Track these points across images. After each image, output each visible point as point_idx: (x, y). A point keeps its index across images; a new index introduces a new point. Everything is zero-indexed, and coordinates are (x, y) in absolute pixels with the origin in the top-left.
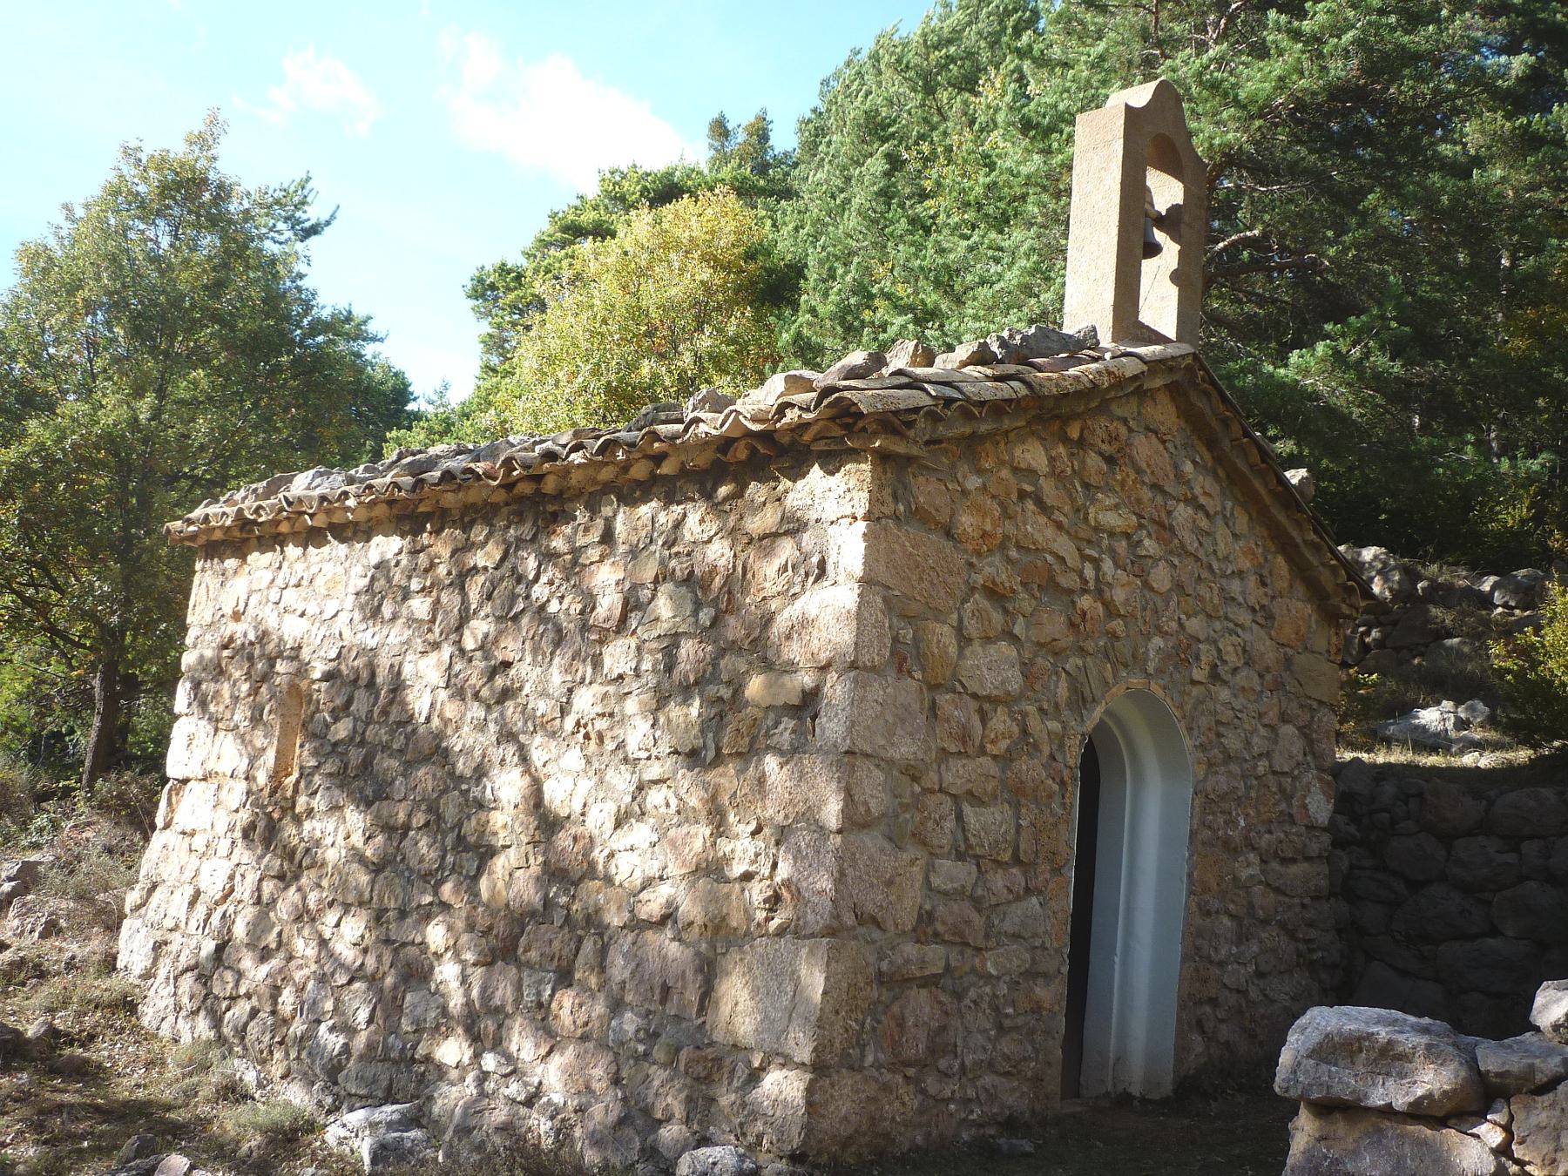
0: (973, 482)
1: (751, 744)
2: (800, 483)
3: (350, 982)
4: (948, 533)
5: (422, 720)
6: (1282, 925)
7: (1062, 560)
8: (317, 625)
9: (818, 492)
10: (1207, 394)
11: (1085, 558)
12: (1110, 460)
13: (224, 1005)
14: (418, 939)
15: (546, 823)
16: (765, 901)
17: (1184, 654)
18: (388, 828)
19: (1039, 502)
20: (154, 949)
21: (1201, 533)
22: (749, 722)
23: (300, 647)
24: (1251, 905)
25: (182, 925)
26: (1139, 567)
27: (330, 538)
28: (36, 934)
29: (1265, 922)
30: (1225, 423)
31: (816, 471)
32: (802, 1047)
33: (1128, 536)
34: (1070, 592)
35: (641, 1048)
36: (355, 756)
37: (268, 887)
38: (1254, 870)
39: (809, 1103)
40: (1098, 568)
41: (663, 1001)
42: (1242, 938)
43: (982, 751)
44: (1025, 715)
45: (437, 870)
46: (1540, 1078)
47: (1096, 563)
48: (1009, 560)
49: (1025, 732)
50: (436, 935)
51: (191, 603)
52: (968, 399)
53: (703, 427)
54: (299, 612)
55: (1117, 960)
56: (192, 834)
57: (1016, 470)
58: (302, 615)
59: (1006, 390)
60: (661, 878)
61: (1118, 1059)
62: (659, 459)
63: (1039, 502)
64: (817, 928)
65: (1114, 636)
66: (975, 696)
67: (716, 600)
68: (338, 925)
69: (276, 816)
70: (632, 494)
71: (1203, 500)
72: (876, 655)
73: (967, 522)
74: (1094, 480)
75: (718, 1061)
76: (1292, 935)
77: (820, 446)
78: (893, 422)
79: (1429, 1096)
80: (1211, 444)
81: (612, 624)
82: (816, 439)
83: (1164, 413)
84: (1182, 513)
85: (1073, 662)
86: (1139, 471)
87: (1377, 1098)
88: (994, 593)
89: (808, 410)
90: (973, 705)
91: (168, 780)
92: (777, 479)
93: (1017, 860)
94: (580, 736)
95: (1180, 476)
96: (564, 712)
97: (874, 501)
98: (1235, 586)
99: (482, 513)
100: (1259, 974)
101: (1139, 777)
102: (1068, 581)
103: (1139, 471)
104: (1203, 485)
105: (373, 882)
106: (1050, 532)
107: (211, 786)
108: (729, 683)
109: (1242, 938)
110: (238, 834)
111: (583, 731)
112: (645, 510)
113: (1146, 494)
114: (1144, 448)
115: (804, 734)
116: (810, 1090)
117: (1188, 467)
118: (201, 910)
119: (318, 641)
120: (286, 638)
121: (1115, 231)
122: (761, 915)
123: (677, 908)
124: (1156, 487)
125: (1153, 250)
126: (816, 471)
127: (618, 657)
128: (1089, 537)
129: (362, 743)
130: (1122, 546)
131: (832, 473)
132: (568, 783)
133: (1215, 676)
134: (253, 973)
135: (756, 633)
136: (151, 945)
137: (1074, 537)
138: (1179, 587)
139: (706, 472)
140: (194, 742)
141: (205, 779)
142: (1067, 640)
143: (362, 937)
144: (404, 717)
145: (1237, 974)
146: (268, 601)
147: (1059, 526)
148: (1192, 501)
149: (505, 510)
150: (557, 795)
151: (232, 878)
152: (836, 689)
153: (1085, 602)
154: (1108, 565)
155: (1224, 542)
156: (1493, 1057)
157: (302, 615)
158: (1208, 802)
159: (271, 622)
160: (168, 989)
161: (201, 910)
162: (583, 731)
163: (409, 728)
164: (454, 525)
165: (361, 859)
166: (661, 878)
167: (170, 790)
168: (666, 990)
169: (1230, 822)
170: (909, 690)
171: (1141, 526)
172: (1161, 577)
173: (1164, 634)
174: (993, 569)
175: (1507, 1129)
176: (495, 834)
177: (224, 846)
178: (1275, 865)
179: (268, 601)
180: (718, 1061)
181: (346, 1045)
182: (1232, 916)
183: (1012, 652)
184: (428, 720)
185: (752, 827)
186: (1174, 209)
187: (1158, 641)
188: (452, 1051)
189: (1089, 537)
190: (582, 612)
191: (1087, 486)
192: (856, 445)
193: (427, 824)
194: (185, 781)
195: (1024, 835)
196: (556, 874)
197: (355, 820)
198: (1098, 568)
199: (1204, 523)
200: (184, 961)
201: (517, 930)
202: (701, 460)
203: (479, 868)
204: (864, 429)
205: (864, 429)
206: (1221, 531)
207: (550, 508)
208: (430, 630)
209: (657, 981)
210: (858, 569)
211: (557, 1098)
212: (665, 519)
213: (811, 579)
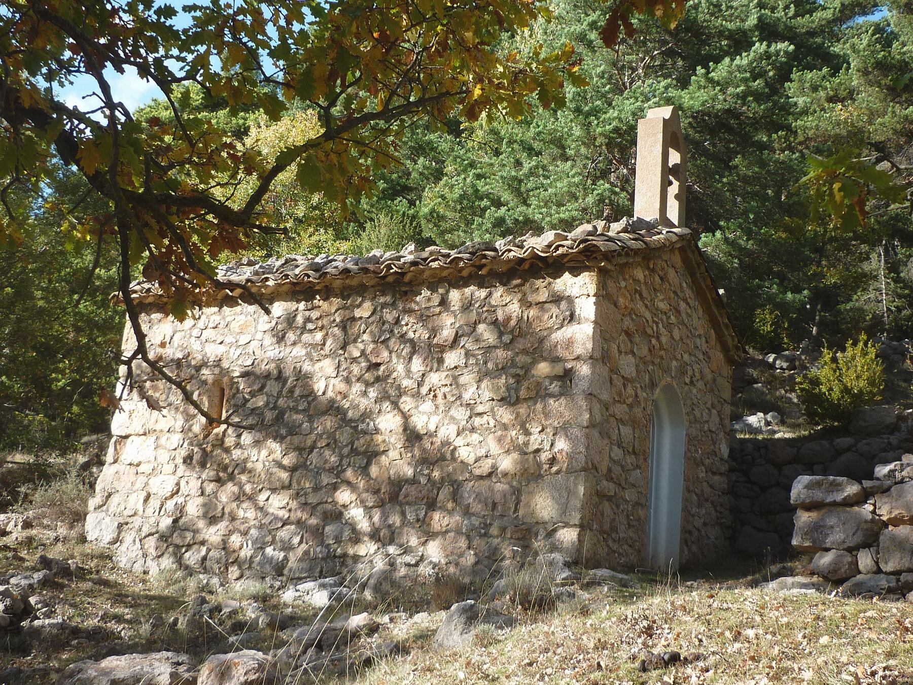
0: (623, 284)
1: (537, 393)
2: (558, 281)
3: (282, 526)
4: (616, 306)
5: (320, 393)
6: (712, 503)
7: (647, 321)
8: (233, 348)
9: (568, 284)
10: (693, 252)
11: (654, 321)
12: (661, 279)
13: (184, 550)
14: (330, 500)
15: (412, 437)
16: (549, 460)
17: (682, 371)
18: (299, 449)
19: (641, 295)
20: (118, 527)
21: (689, 316)
22: (535, 384)
23: (220, 360)
24: (702, 491)
25: (140, 512)
26: (669, 327)
27: (240, 302)
28: (19, 527)
29: (707, 500)
30: (699, 265)
31: (567, 275)
32: (576, 518)
33: (666, 314)
34: (649, 336)
35: (483, 531)
36: (269, 416)
37: (210, 487)
38: (703, 475)
39: (579, 541)
40: (657, 327)
41: (493, 510)
42: (700, 506)
43: (624, 403)
44: (636, 388)
45: (338, 466)
46: (885, 487)
47: (657, 323)
48: (632, 319)
49: (636, 396)
50: (344, 496)
51: (124, 339)
52: (628, 247)
53: (512, 253)
54: (219, 342)
55: (652, 511)
56: (138, 465)
57: (634, 280)
58: (221, 343)
59: (638, 245)
60: (487, 456)
61: (653, 557)
62: (481, 267)
63: (641, 295)
64: (578, 468)
65: (662, 358)
66: (623, 377)
67: (512, 332)
68: (267, 499)
69: (209, 449)
70: (460, 282)
71: (689, 300)
72: (598, 355)
73: (621, 301)
74: (657, 287)
75: (529, 530)
76: (715, 507)
77: (572, 264)
78: (608, 256)
79: (849, 496)
80: (692, 275)
81: (449, 343)
82: (568, 261)
83: (677, 259)
84: (683, 305)
85: (651, 368)
86: (670, 285)
87: (829, 499)
88: (627, 333)
89: (572, 248)
90: (622, 381)
91: (112, 436)
92: (544, 278)
93: (634, 452)
94: (431, 396)
95: (681, 287)
96: (420, 385)
97: (598, 289)
98: (698, 341)
99: (361, 290)
100: (705, 524)
101: (661, 428)
102: (649, 331)
103: (670, 285)
104: (688, 293)
105: (291, 477)
106: (644, 308)
107: (151, 439)
108: (522, 368)
109: (700, 506)
110: (179, 461)
111: (432, 393)
112: (468, 291)
113: (672, 295)
114: (672, 274)
115: (566, 387)
116: (579, 535)
117: (684, 285)
118: (154, 503)
119: (236, 357)
120: (208, 355)
121: (660, 175)
122: (546, 467)
123: (497, 469)
124: (675, 293)
125: (671, 183)
126: (567, 275)
127: (452, 358)
128: (655, 312)
129: (275, 407)
130: (664, 318)
131: (576, 276)
132: (425, 418)
133: (692, 382)
134: (205, 530)
135: (536, 345)
136: (116, 524)
137: (651, 312)
138: (681, 339)
139: (503, 273)
140: (133, 415)
141: (145, 434)
142: (648, 358)
143: (288, 504)
144: (305, 393)
145: (698, 522)
146: (191, 336)
147: (646, 306)
148: (685, 300)
149: (372, 290)
150: (420, 422)
151: (178, 484)
152: (584, 370)
153: (654, 341)
154: (660, 326)
155: (695, 322)
156: (867, 484)
157: (221, 343)
158: (690, 439)
159: (196, 346)
160: (136, 547)
161: (154, 503)
162: (432, 393)
163: (310, 399)
164: (336, 296)
165: (280, 466)
166: (487, 456)
167: (115, 442)
168: (494, 505)
169: (697, 451)
170: (604, 370)
171: (670, 310)
172: (676, 334)
173: (677, 360)
174: (628, 323)
175: (874, 505)
176: (378, 445)
177: (169, 468)
178: (710, 474)
179: (191, 336)
180: (529, 530)
181: (285, 556)
182: (696, 494)
183: (633, 360)
184: (324, 393)
185: (540, 428)
186: (675, 165)
187: (674, 363)
188: (367, 548)
189: (655, 312)
190: (429, 338)
191: (655, 289)
192: (591, 264)
193: (328, 445)
194: (127, 437)
195: (637, 440)
196: (426, 461)
197: (276, 447)
198: (657, 327)
199: (689, 311)
200: (145, 530)
201: (397, 489)
202: (503, 269)
203: (367, 463)
204: (596, 258)
205: (596, 258)
206: (694, 316)
207: (404, 289)
208: (322, 349)
209: (490, 501)
210: (593, 318)
211: (435, 560)
212: (483, 293)
213: (566, 322)
